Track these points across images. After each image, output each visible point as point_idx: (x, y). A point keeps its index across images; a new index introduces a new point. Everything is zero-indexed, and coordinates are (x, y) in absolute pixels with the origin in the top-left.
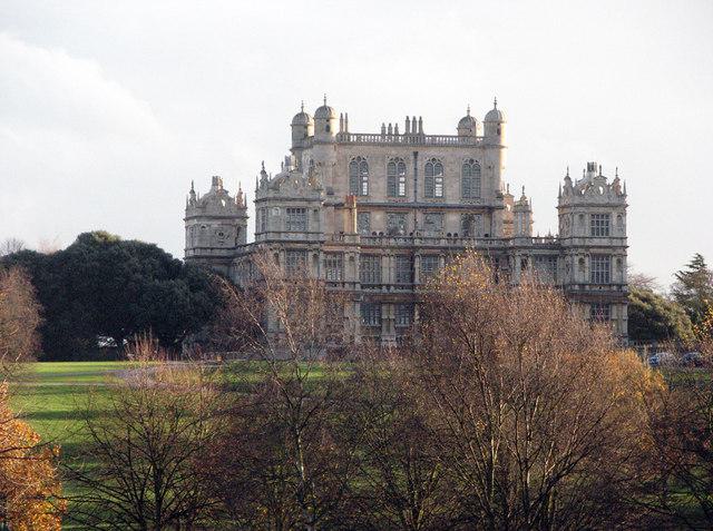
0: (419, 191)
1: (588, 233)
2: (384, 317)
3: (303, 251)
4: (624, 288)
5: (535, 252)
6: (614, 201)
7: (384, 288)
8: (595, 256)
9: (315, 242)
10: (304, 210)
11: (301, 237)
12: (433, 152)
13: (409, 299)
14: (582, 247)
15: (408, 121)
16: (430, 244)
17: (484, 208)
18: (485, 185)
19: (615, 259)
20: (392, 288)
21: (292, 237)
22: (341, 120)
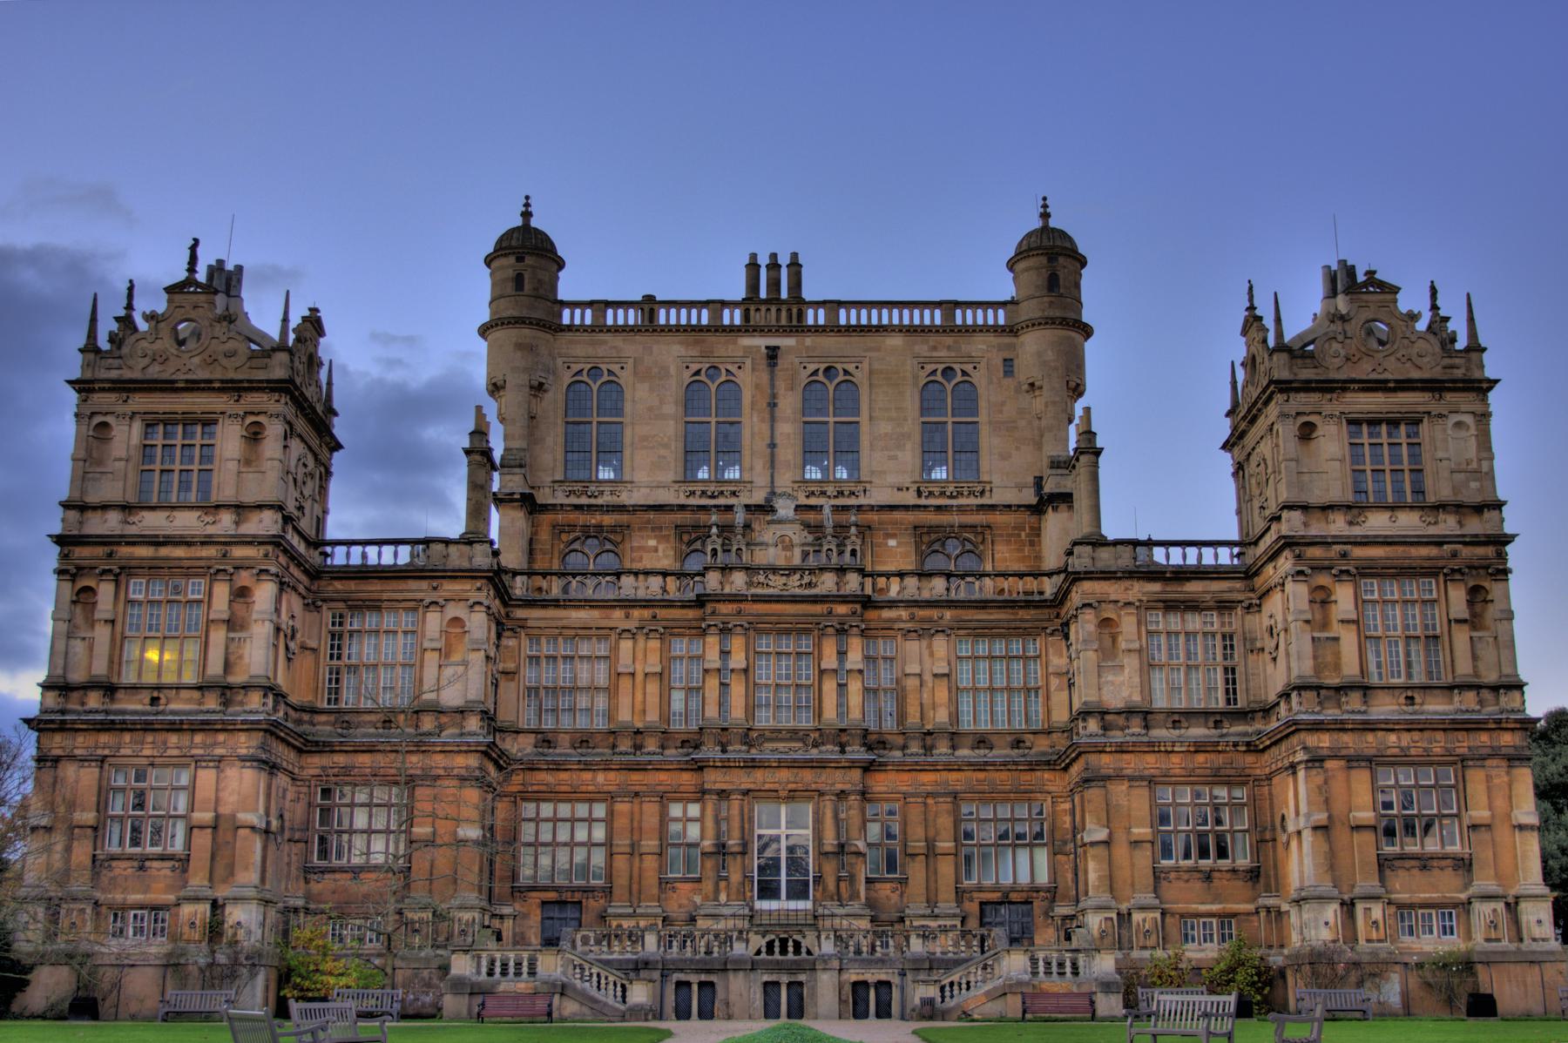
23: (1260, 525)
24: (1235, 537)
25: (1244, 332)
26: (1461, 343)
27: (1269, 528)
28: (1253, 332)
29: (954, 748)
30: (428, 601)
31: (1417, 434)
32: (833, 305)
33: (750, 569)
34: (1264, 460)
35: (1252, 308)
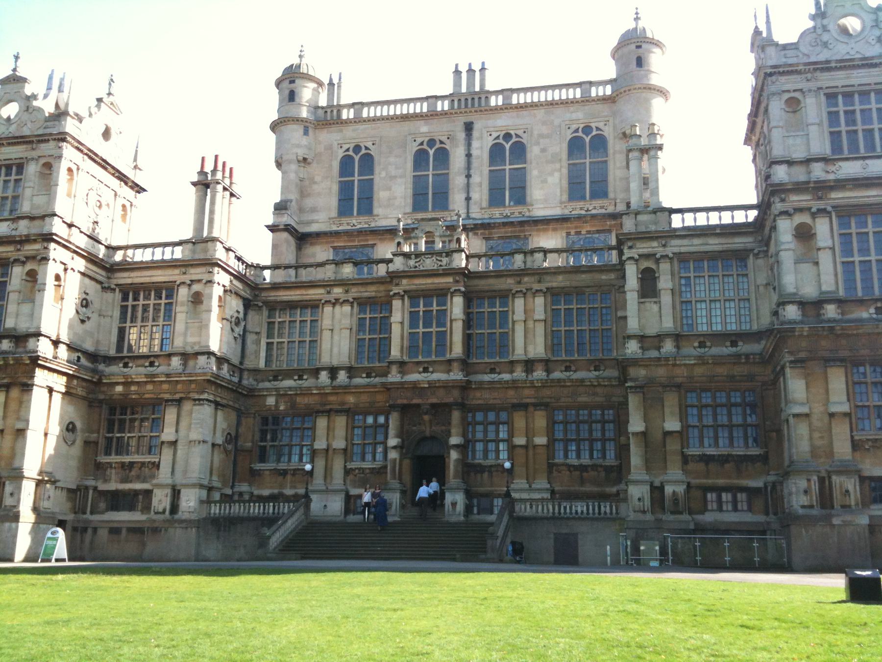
0: (475, 196)
1: (820, 145)
2: (320, 444)
5: (676, 246)
7: (324, 376)
8: (845, 213)
9: (27, 240)
10: (20, 168)
14: (799, 188)
15: (457, 73)
16: (429, 264)
20: (342, 376)
22: (331, 84)
29: (548, 371)
30: (178, 283)
32: (507, 92)
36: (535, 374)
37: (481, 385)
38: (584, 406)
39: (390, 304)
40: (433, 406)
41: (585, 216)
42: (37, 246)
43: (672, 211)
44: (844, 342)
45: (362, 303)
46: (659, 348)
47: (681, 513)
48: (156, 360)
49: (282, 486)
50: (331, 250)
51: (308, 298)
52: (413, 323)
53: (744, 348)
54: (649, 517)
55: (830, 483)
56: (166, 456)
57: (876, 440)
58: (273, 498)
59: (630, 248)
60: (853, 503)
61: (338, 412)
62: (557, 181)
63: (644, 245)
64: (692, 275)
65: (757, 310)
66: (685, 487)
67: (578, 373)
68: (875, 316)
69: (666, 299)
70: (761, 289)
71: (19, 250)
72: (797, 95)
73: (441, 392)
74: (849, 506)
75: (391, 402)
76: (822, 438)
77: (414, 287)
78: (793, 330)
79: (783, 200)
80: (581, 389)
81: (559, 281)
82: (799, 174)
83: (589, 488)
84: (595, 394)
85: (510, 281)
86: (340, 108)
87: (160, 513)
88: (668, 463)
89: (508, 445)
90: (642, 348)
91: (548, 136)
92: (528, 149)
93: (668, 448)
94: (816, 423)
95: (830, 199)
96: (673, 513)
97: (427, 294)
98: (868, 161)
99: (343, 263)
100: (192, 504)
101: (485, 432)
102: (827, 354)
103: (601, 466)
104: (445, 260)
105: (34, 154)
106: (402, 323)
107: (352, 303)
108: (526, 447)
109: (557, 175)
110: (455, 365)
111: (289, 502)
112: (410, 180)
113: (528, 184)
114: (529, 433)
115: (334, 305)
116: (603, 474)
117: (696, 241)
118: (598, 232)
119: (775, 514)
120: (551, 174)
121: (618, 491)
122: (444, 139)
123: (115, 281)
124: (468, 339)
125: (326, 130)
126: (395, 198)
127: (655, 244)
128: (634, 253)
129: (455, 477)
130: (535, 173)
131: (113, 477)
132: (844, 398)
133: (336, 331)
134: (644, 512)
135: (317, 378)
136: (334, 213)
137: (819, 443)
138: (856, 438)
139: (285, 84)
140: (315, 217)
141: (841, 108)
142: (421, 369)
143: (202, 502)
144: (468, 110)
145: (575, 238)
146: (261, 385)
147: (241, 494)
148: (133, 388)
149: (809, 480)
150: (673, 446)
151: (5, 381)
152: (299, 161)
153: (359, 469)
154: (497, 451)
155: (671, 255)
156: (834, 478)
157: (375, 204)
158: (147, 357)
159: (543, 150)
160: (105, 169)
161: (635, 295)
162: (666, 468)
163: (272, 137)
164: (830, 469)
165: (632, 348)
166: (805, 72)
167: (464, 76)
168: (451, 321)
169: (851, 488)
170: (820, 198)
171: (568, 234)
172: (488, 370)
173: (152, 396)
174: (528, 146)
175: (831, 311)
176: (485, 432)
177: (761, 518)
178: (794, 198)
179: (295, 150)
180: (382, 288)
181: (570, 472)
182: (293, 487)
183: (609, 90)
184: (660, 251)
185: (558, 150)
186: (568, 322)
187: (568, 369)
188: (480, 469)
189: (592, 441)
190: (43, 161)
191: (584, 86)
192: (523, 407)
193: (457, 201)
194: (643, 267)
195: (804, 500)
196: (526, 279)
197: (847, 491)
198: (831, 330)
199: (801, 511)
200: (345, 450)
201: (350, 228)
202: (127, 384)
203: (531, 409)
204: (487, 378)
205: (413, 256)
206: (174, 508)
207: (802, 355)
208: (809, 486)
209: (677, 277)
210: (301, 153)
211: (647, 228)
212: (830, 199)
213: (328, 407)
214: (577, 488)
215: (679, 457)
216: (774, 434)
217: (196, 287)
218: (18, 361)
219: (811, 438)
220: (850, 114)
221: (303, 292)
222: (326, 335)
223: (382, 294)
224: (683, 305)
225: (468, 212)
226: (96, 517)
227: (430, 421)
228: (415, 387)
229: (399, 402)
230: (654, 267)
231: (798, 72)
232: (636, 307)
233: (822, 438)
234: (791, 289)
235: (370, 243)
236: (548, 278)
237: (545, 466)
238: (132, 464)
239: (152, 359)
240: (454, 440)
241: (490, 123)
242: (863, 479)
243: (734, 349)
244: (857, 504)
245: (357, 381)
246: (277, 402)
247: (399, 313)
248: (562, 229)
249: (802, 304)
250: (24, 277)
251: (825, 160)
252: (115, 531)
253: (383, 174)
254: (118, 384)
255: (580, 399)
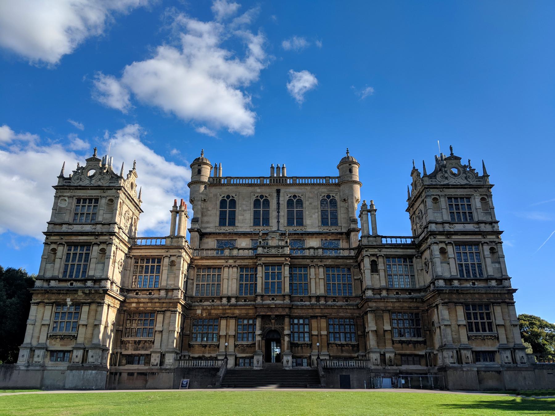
0: (281, 221)
1: (447, 217)
2: (223, 333)
3: (89, 245)
4: (505, 283)
5: (385, 252)
6: (473, 182)
7: (224, 301)
8: (458, 244)
9: (102, 234)
10: (97, 201)
11: (88, 228)
12: (294, 190)
13: (251, 312)
14: (441, 233)
15: (272, 168)
16: (273, 251)
17: (341, 234)
18: (341, 216)
19: (486, 248)
20: (233, 301)
21: (77, 228)
23: (420, 231)
24: (411, 235)
25: (411, 176)
26: (481, 174)
27: (424, 231)
28: (415, 174)
29: (326, 301)
30: (164, 256)
31: (469, 202)
33: (264, 247)
34: (421, 211)
35: (414, 167)
36: (320, 302)
37: (297, 307)
38: (342, 318)
39: (256, 268)
40: (276, 316)
41: (329, 233)
42: (106, 237)
43: (383, 237)
44: (462, 296)
45: (241, 268)
46: (380, 294)
47: (393, 366)
48: (152, 292)
49: (204, 352)
50: (216, 241)
51: (217, 264)
52: (267, 277)
53: (413, 295)
54: (380, 367)
55: (460, 354)
56: (158, 337)
57: (476, 336)
58: (200, 358)
59: (366, 251)
60: (470, 362)
61: (231, 317)
62: (317, 217)
63: (372, 250)
64: (391, 264)
65: (418, 280)
66: (394, 354)
67: (339, 302)
68: (472, 286)
69: (382, 273)
70: (419, 271)
71: (96, 239)
72: (437, 197)
73: (280, 310)
74: (469, 363)
75: (258, 314)
76: (456, 334)
77: (267, 262)
78: (443, 290)
79: (435, 238)
80: (341, 310)
81: (329, 262)
82: (440, 228)
83: (345, 354)
84: (347, 312)
85: (308, 261)
86: (220, 179)
87: (155, 365)
88: (386, 344)
89: (309, 334)
90: (373, 294)
91: (312, 198)
92: (304, 203)
93: (386, 337)
94: (453, 329)
95: (452, 239)
96: (389, 365)
97: (273, 265)
98: (465, 225)
99: (233, 249)
100: (171, 361)
101: (299, 328)
102: (455, 300)
103: (350, 344)
104: (281, 250)
105: (105, 195)
106: (262, 277)
107: (237, 267)
108: (317, 335)
109: (316, 214)
110: (287, 297)
111: (208, 360)
112: (252, 212)
113: (304, 217)
114: (319, 329)
115: (229, 267)
116: (351, 348)
117: (393, 250)
118: (334, 240)
119: (431, 366)
120: (314, 214)
121: (358, 356)
122: (267, 195)
123: (132, 254)
124: (291, 285)
125: (214, 188)
126: (246, 220)
127: (376, 250)
128: (368, 253)
129: (288, 349)
130: (307, 213)
131: (130, 348)
132: (464, 319)
133: (230, 280)
134: (378, 365)
135: (221, 302)
136: (217, 224)
137: (455, 336)
138: (469, 335)
139: (196, 166)
140: (208, 225)
141: (454, 203)
142: (271, 299)
143: (176, 360)
144: (280, 184)
145: (325, 242)
146: (193, 304)
147: (185, 356)
148: (141, 305)
149: (453, 352)
150: (388, 336)
151: (89, 301)
152: (202, 200)
153: (241, 345)
154: (304, 337)
155: (383, 255)
156: (462, 351)
157: (236, 221)
158: (148, 290)
159: (310, 204)
160: (131, 202)
161: (369, 271)
162: (385, 346)
163: (188, 189)
164: (460, 348)
165: (369, 293)
166: (440, 188)
167: (275, 169)
168: (284, 277)
169: (469, 355)
170: (448, 238)
171: (322, 240)
172: (299, 300)
173: (151, 309)
174: (304, 201)
175: (456, 283)
176: (299, 328)
177: (425, 368)
178: (439, 237)
179: (201, 196)
180: (251, 261)
181: (337, 346)
182: (209, 353)
183: (337, 181)
184: (379, 253)
185: (317, 204)
186: (334, 280)
187: (334, 301)
188: (297, 345)
189: (346, 333)
190: (108, 198)
191: (327, 178)
192: (316, 317)
193: (273, 221)
194: (371, 260)
195: (452, 360)
196: (315, 260)
197: (468, 357)
198: (458, 292)
199: (451, 365)
200: (235, 336)
201: (225, 231)
202: (138, 303)
203: (319, 318)
204: (299, 303)
205: (266, 248)
206: (162, 363)
207: (446, 300)
208: (453, 355)
209: (386, 264)
210: (203, 197)
211: (372, 243)
212: (452, 239)
213: (227, 315)
214: (340, 354)
215: (391, 341)
216: (428, 332)
217: (173, 258)
218: (97, 292)
219: (452, 335)
220: (457, 205)
221: (214, 261)
222: (225, 281)
223: (252, 264)
224: (389, 276)
225: (278, 228)
226: (121, 367)
227: (274, 323)
228: (269, 307)
229: (261, 314)
230: (376, 260)
231: (437, 188)
232: (370, 276)
233: (456, 334)
234: (440, 274)
235: (234, 238)
236: (325, 260)
237: (326, 344)
238: (140, 342)
239: (150, 291)
240: (286, 332)
241: (287, 190)
242: (473, 352)
243: (410, 296)
244: (472, 362)
245: (240, 303)
246: (202, 312)
247: (260, 272)
248: (319, 237)
249: (445, 280)
250: (99, 252)
251: (449, 223)
252: (131, 374)
253: (240, 209)
254: (133, 302)
255: (340, 314)
